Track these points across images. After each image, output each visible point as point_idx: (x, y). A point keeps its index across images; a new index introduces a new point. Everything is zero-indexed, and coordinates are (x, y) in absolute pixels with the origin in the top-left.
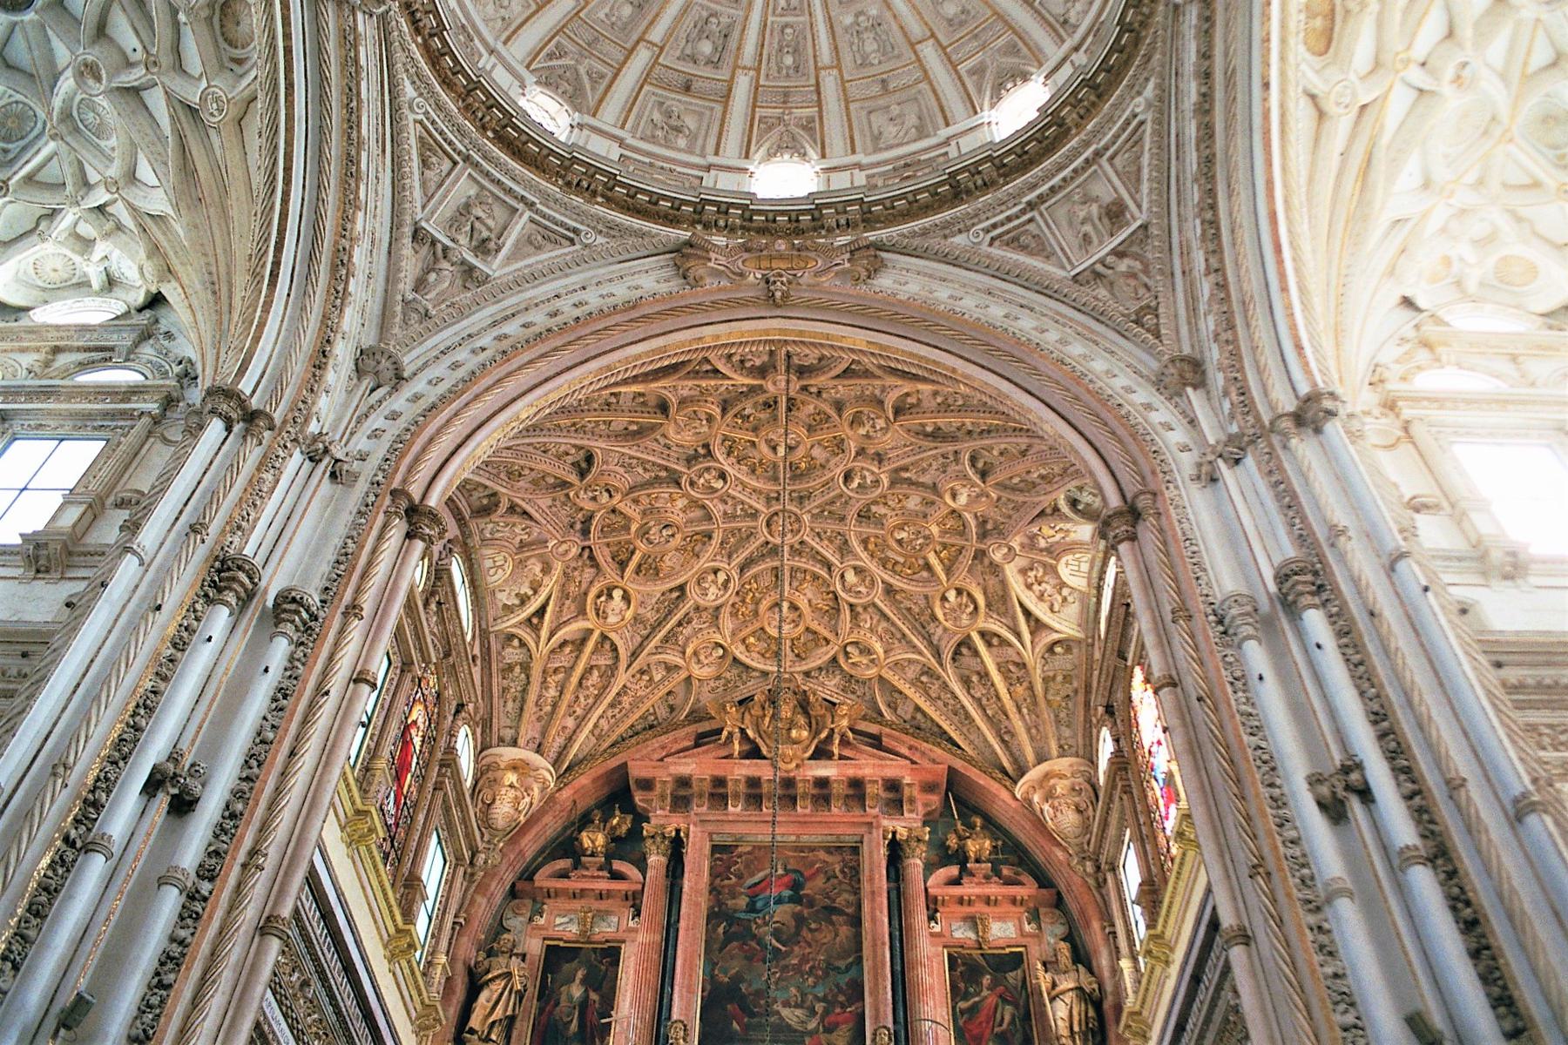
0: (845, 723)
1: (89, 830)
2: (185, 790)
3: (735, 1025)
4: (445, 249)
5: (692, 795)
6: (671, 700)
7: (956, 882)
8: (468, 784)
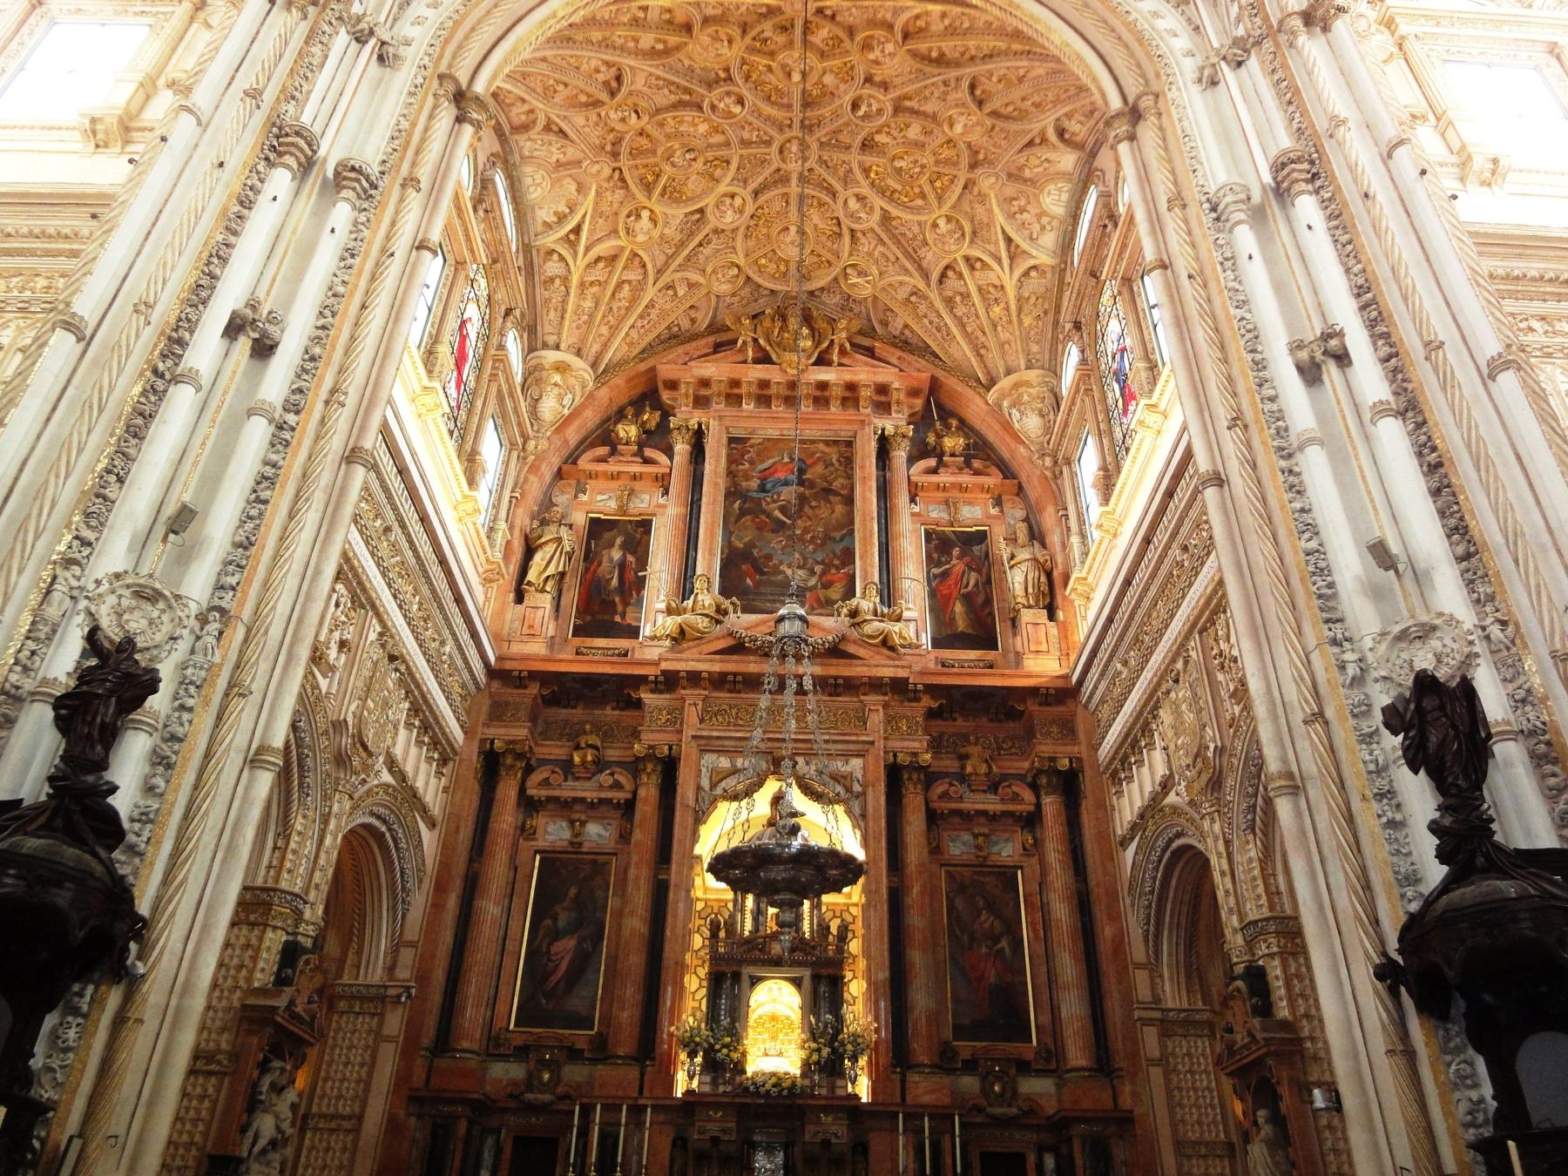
0: (844, 335)
1: (176, 365)
2: (265, 334)
3: (748, 581)
6: (693, 313)
7: (934, 471)
8: (519, 379)
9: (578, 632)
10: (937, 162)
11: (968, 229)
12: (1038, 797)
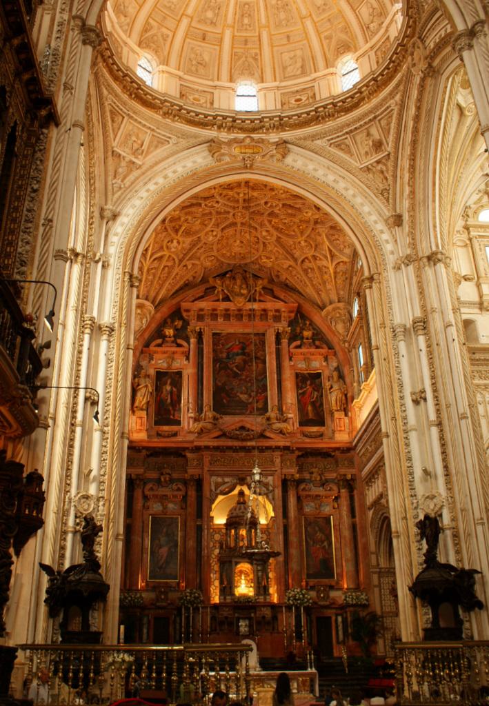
2: (94, 400)
4: (124, 157)
5: (205, 314)
6: (194, 275)
9: (156, 423)
10: (301, 221)
12: (339, 490)
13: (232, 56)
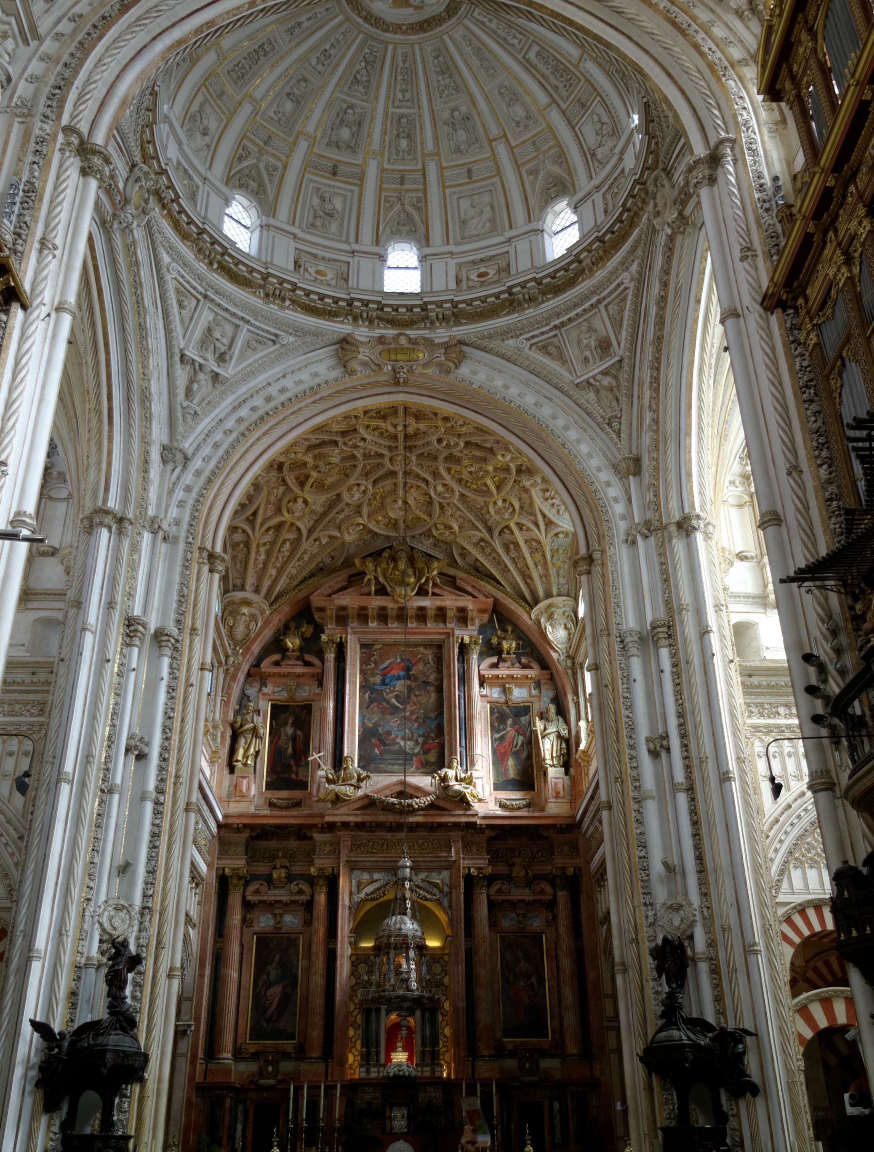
4: (201, 365)
11: (517, 505)
13: (380, 201)
